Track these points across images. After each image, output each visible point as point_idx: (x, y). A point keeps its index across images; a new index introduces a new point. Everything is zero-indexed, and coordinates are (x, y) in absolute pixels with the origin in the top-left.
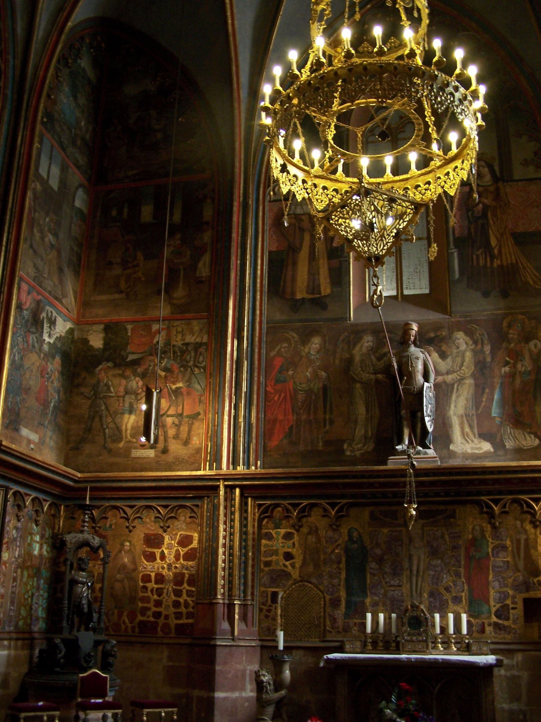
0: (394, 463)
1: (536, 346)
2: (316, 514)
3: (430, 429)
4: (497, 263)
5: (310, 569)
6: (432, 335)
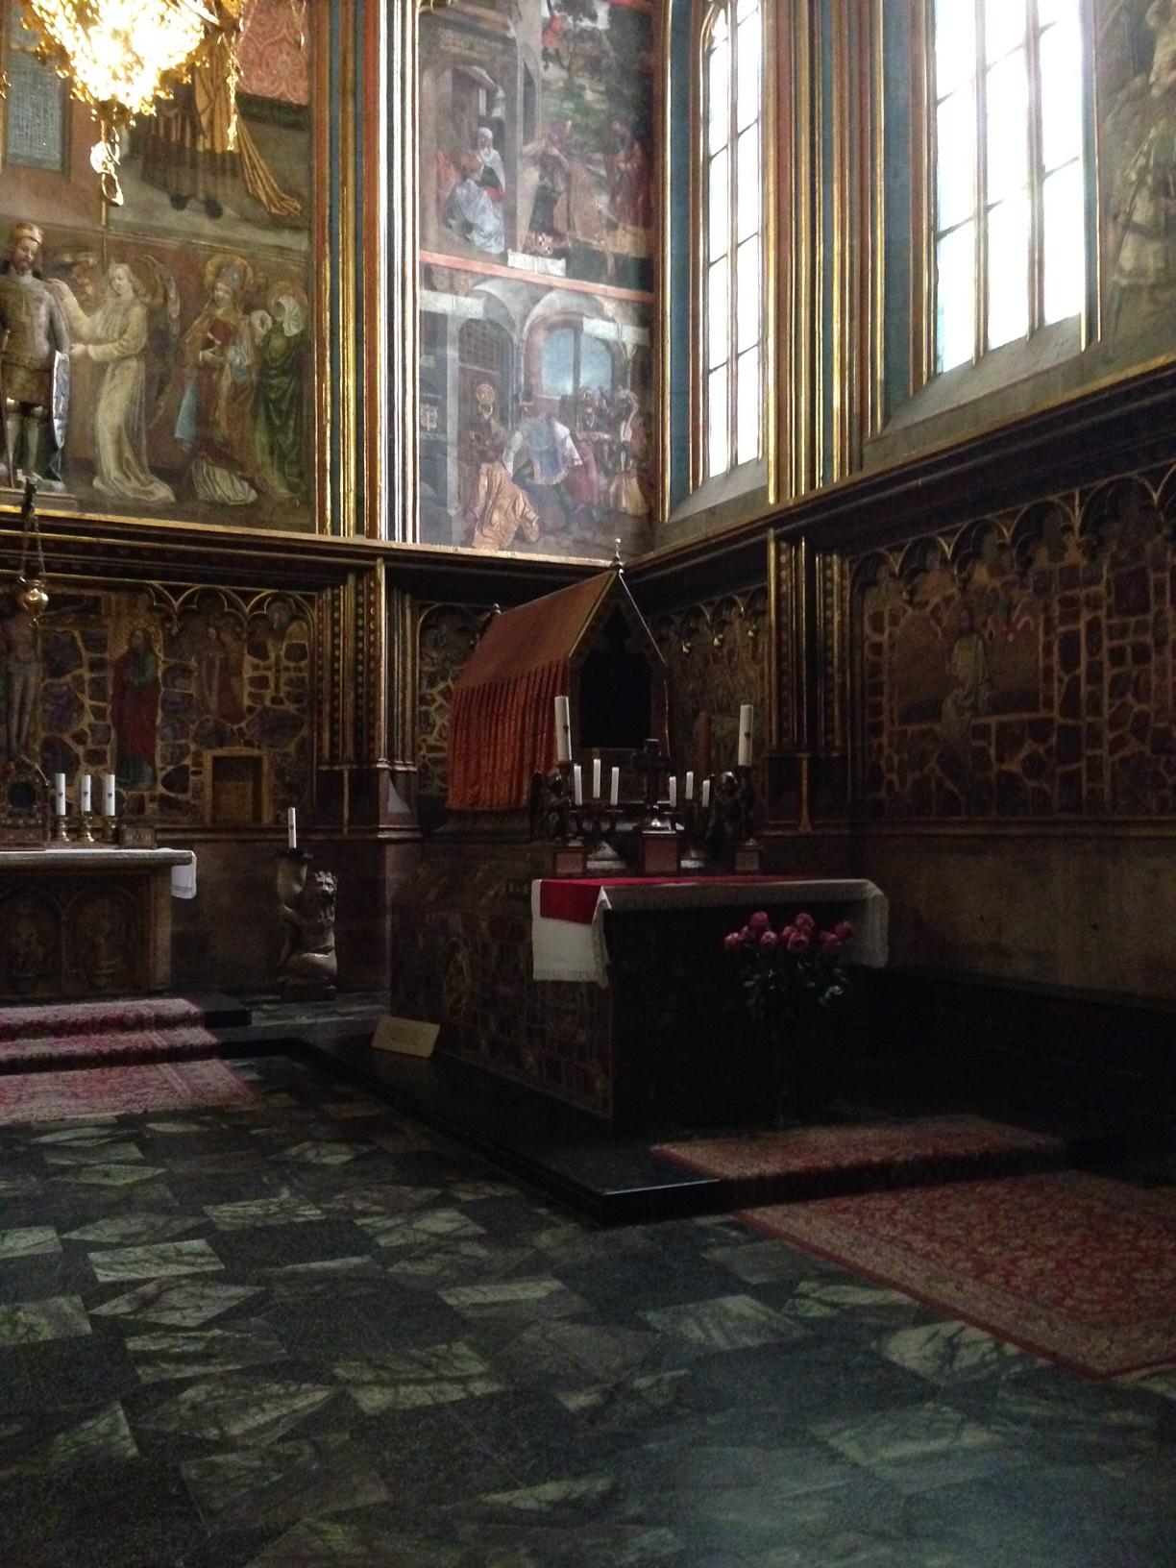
1: (263, 322)
3: (60, 444)
4: (203, 144)
6: (68, 259)
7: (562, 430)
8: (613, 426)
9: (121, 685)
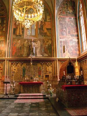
0: (29, 58)
2: (19, 64)
5: (18, 71)
7: (72, 48)
8: (76, 47)
9: (39, 70)
